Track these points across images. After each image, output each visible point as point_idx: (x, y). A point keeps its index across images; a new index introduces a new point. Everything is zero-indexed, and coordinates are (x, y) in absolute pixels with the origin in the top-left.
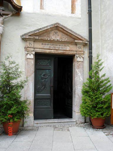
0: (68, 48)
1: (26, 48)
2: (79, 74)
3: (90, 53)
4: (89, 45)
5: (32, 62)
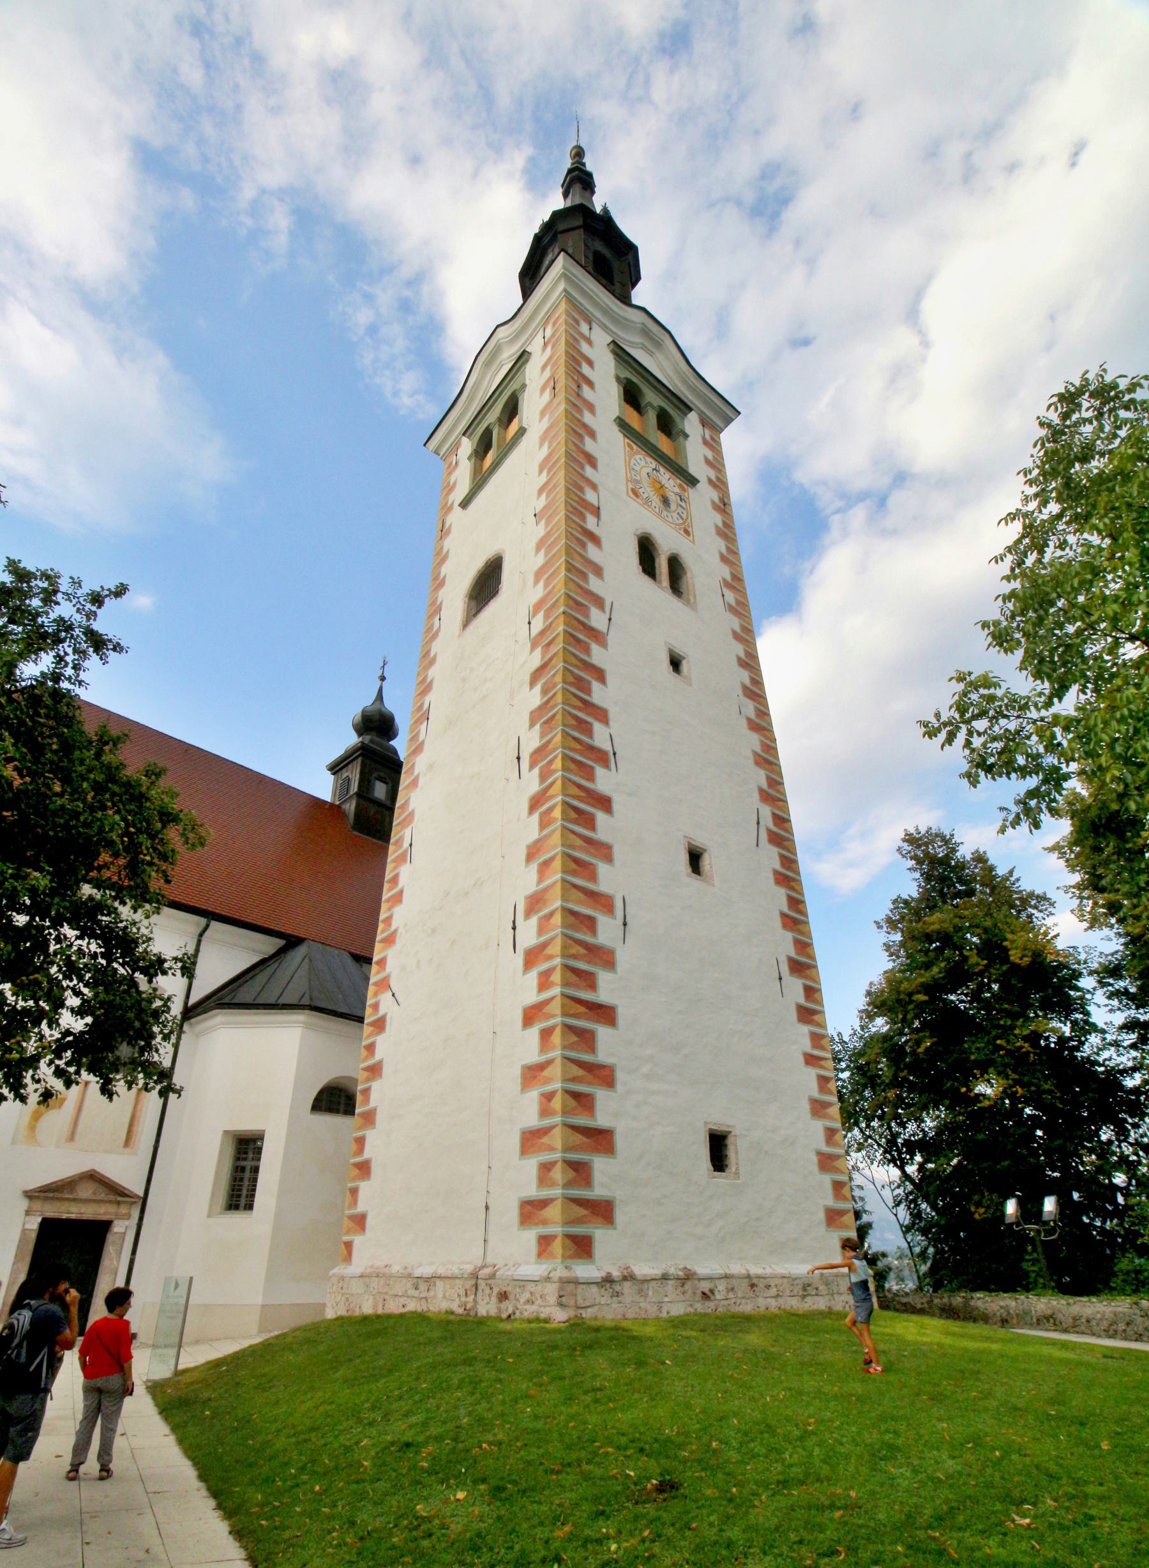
1: (28, 1213)
3: (141, 1219)
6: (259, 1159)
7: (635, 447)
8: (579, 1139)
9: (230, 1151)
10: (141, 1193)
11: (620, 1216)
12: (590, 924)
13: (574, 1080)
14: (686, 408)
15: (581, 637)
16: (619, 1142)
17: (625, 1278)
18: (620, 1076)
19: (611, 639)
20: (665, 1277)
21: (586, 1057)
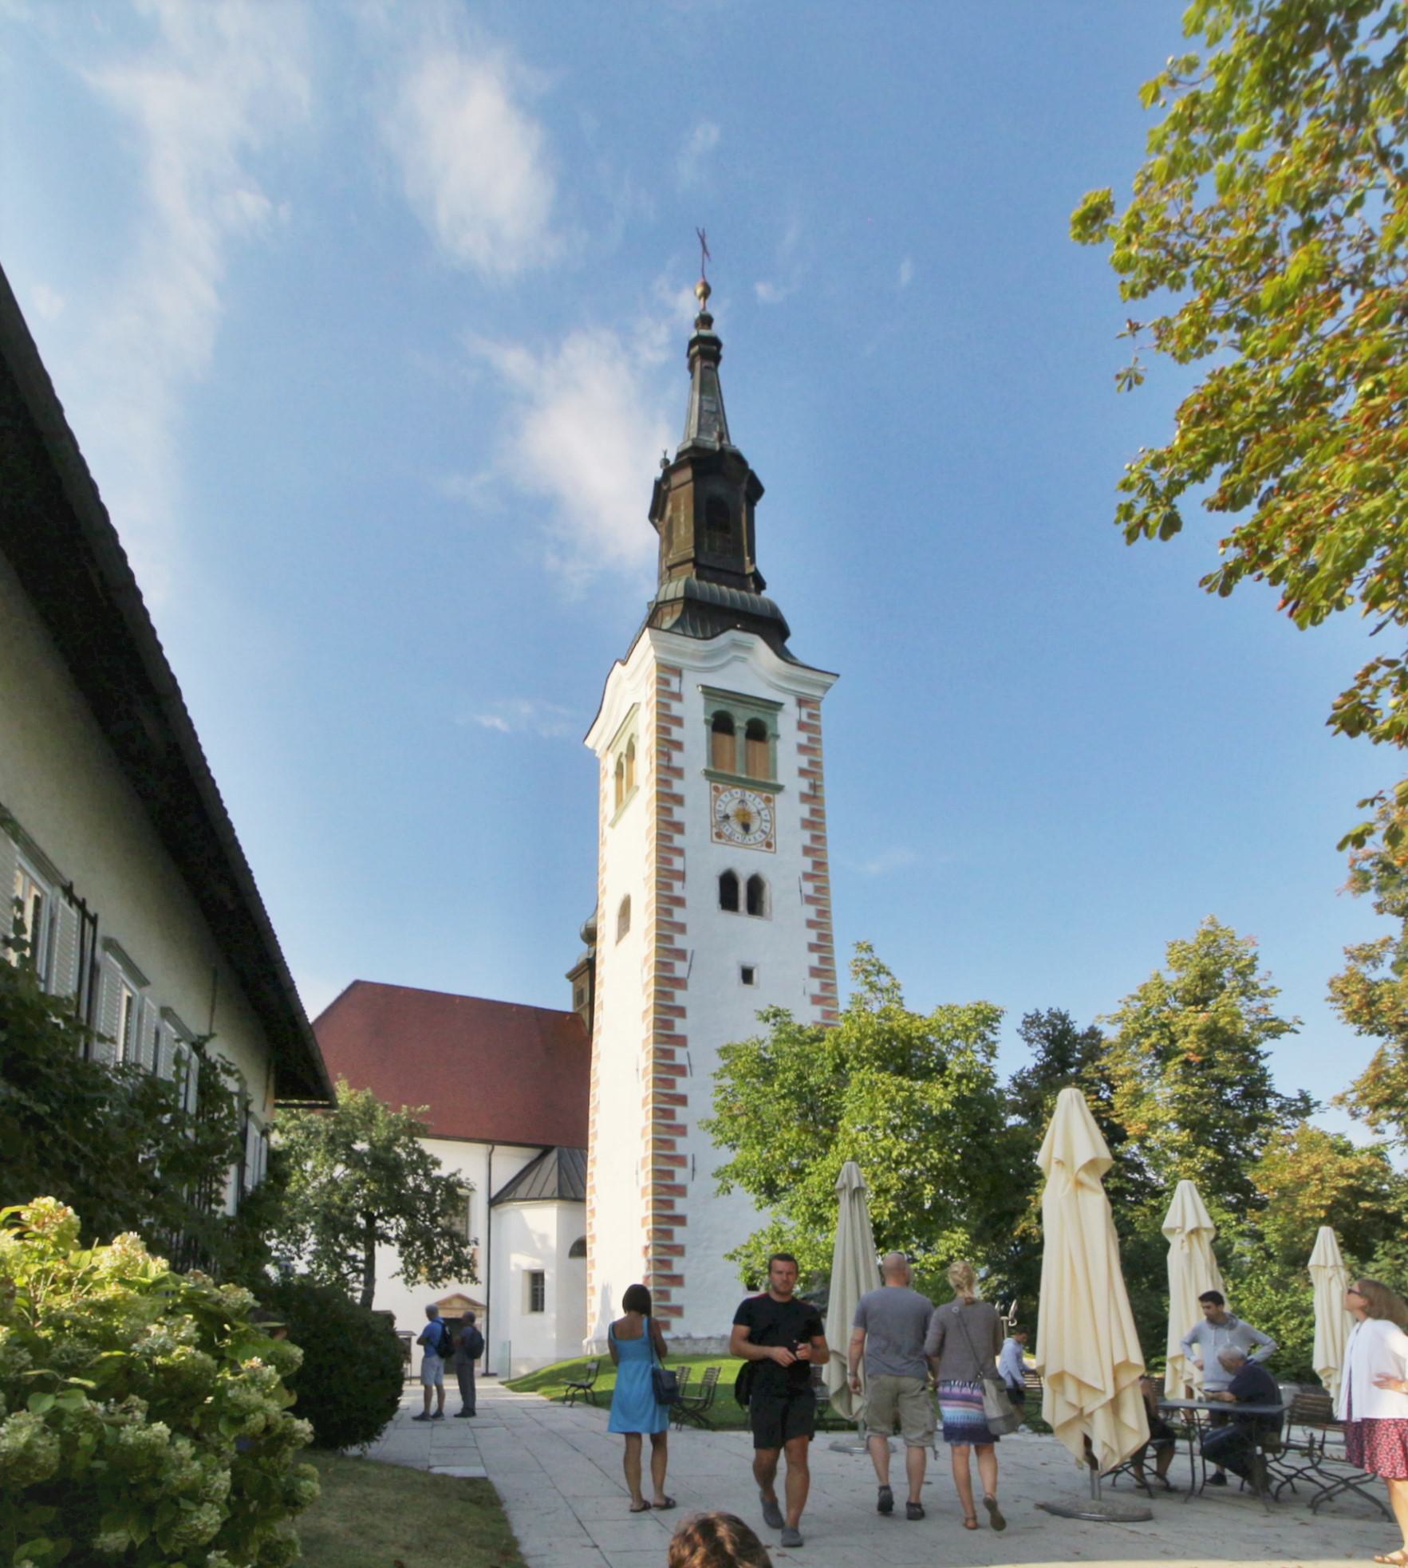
7: (720, 786)
8: (663, 1280)
11: (686, 1312)
12: (670, 1174)
13: (661, 1254)
15: (667, 989)
16: (687, 1280)
17: (685, 1338)
18: (688, 1250)
19: (691, 982)
20: (710, 1338)
21: (667, 1242)
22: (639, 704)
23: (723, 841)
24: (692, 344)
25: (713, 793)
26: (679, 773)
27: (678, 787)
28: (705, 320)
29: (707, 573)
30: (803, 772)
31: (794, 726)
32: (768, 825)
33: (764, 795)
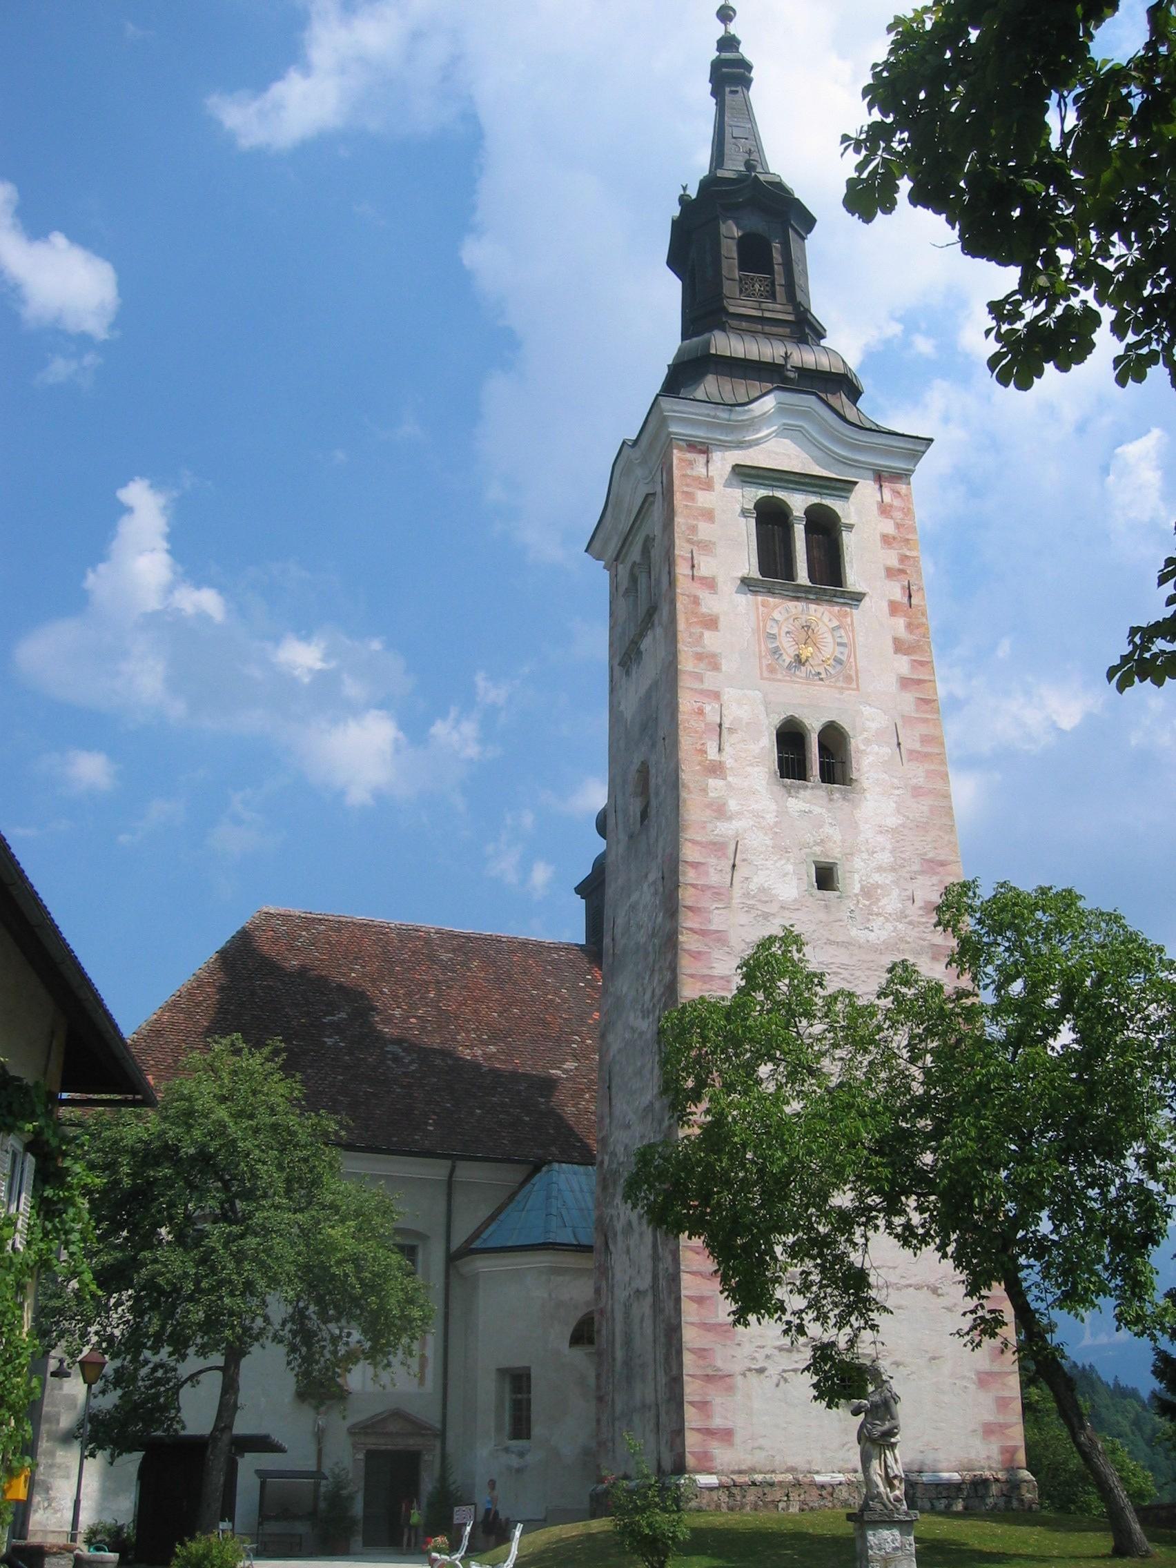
0: (411, 1442)
1: (354, 1446)
2: (427, 1480)
3: (443, 1449)
4: (442, 1435)
5: (362, 1464)
6: (529, 1392)
9: (507, 1387)
10: (438, 1426)
14: (844, 488)
22: (654, 494)
23: (779, 676)
24: (717, 66)
25: (760, 607)
26: (710, 584)
27: (711, 604)
28: (727, 43)
29: (744, 325)
30: (891, 573)
31: (875, 509)
32: (846, 651)
33: (836, 608)
